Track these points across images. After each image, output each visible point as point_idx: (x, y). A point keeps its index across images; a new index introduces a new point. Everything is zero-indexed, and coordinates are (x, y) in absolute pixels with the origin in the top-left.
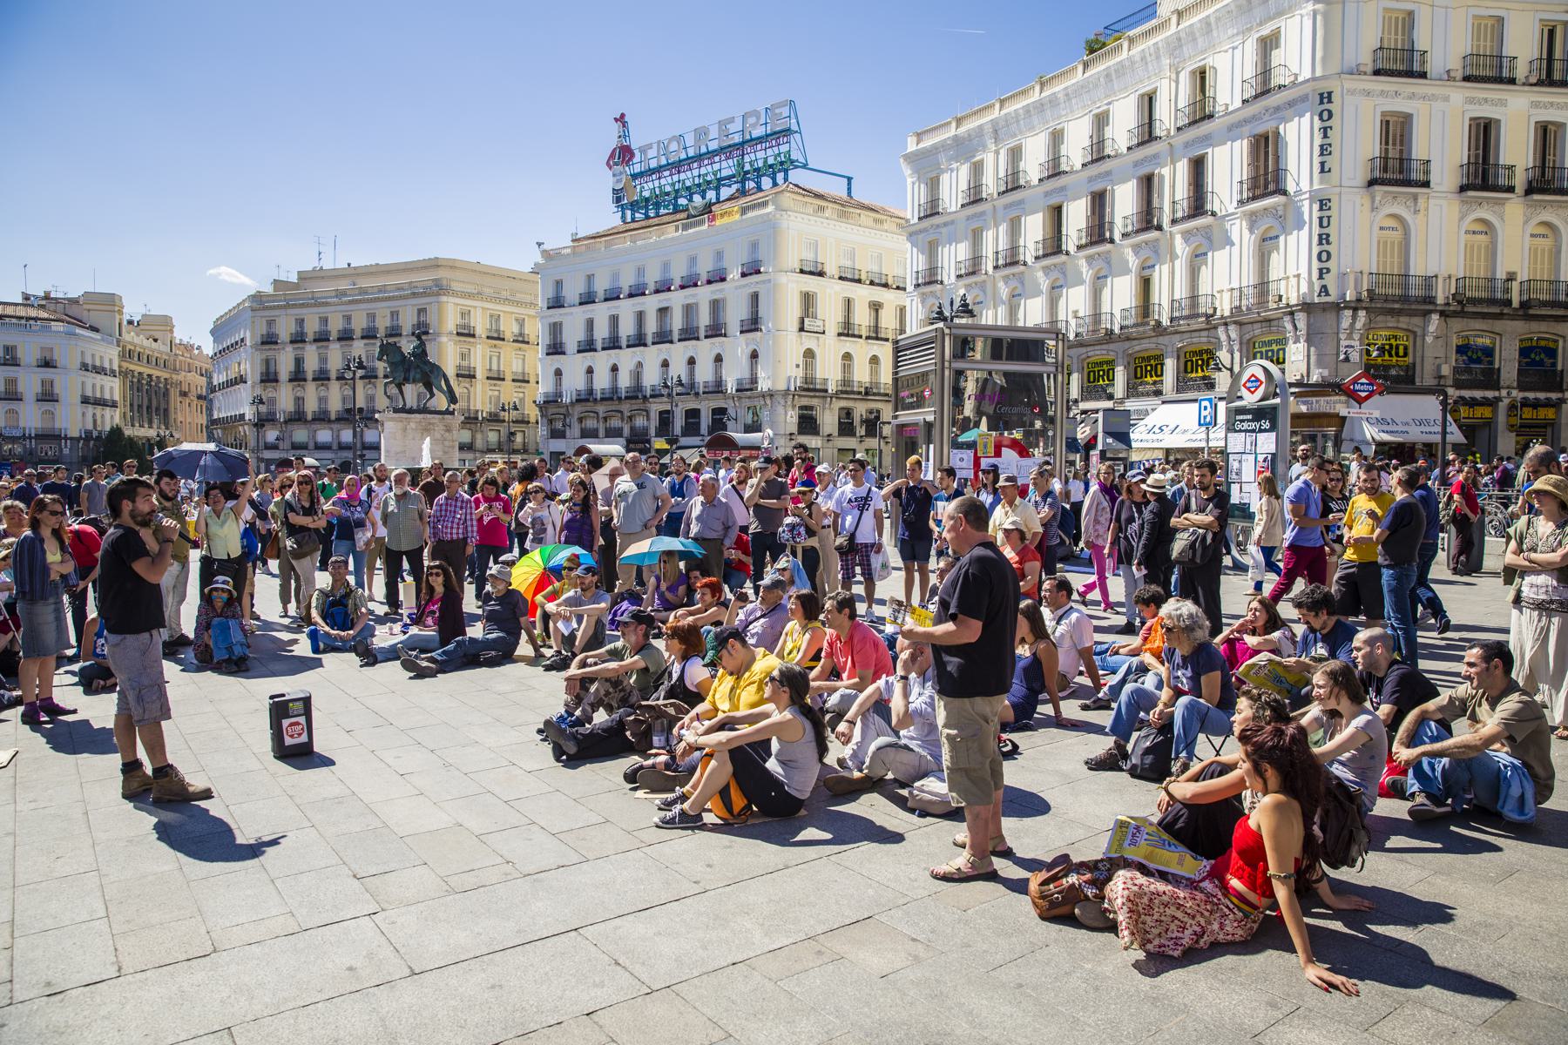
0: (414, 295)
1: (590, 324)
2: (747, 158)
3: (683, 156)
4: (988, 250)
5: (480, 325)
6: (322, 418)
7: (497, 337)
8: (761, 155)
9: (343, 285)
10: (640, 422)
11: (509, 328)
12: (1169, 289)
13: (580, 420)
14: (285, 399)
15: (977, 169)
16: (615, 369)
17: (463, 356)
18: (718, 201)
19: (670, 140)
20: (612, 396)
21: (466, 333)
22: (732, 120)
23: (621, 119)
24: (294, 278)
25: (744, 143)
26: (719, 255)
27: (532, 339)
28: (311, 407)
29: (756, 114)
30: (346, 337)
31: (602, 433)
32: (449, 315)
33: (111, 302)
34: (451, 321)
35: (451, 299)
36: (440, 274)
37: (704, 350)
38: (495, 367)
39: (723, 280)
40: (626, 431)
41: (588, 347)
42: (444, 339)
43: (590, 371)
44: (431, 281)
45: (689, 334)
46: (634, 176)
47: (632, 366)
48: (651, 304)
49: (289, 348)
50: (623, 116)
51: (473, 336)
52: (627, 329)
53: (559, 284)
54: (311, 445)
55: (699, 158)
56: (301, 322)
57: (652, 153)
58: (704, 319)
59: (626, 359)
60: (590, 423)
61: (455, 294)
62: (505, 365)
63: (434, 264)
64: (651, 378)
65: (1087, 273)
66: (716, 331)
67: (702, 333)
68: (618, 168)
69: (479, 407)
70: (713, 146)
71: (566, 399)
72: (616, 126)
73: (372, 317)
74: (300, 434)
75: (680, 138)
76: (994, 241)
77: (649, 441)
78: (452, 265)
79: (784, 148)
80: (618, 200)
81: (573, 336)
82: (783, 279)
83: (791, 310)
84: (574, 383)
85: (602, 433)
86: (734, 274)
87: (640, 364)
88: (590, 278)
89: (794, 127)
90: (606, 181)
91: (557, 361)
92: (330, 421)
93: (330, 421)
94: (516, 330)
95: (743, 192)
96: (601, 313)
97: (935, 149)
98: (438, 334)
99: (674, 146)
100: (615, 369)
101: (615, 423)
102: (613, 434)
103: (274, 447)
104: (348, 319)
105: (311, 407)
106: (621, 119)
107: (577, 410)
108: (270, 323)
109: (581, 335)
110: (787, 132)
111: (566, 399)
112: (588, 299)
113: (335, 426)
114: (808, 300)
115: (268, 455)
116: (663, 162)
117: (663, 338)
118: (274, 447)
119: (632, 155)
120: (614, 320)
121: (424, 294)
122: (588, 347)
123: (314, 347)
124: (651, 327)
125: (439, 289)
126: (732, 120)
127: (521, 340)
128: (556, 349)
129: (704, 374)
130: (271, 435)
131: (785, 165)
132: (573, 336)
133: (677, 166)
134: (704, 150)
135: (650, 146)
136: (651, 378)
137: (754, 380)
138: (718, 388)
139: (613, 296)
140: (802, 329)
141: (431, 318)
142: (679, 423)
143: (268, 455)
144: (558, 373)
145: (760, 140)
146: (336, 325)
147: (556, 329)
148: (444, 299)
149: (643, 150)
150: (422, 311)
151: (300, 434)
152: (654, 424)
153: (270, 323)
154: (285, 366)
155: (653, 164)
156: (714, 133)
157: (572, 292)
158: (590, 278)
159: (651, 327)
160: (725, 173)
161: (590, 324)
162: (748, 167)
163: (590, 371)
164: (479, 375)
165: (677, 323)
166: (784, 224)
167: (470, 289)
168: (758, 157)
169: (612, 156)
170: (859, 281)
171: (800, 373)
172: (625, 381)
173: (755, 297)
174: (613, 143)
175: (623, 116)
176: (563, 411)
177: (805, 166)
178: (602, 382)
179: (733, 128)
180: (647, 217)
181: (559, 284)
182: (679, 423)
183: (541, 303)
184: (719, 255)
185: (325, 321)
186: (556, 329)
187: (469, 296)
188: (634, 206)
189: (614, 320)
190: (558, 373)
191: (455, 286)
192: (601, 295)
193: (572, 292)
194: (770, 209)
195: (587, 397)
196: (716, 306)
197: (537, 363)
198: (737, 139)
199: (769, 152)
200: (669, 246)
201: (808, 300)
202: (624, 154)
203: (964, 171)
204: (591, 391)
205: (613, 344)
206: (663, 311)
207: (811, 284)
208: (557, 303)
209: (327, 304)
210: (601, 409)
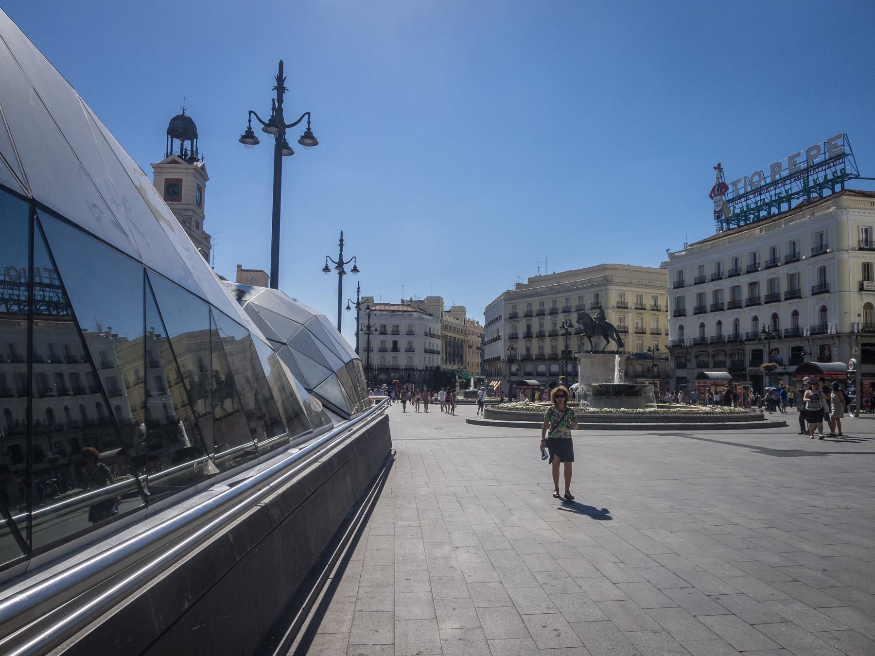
0: (592, 286)
2: (811, 178)
3: (763, 183)
5: (631, 301)
6: (541, 358)
7: (641, 308)
8: (823, 173)
9: (553, 284)
11: (648, 302)
13: (697, 357)
14: (521, 348)
19: (753, 175)
20: (718, 341)
23: (719, 168)
24: (526, 282)
25: (807, 168)
27: (663, 308)
28: (535, 352)
29: (817, 148)
30: (554, 312)
31: (711, 365)
35: (613, 287)
36: (607, 273)
37: (785, 310)
38: (640, 326)
40: (728, 363)
41: (700, 310)
42: (610, 311)
43: (702, 325)
44: (601, 277)
45: (773, 298)
46: (729, 201)
47: (732, 320)
49: (524, 320)
50: (719, 165)
51: (627, 308)
53: (681, 273)
54: (535, 373)
55: (775, 183)
58: (784, 288)
59: (728, 318)
61: (616, 284)
63: (603, 268)
64: (746, 328)
66: (794, 294)
67: (783, 297)
68: (718, 198)
70: (785, 173)
74: (529, 367)
75: (759, 173)
77: (745, 370)
78: (613, 267)
81: (690, 305)
84: (692, 333)
85: (711, 365)
88: (701, 267)
89: (848, 151)
90: (710, 206)
91: (681, 321)
92: (545, 360)
93: (545, 360)
94: (652, 303)
96: (709, 288)
101: (721, 358)
102: (718, 366)
103: (515, 374)
104: (555, 302)
105: (535, 352)
108: (514, 307)
110: (842, 156)
111: (687, 343)
112: (700, 281)
113: (548, 363)
116: (749, 189)
118: (515, 374)
119: (727, 188)
121: (598, 286)
122: (700, 310)
123: (537, 319)
125: (607, 282)
127: (656, 308)
128: (679, 313)
129: (785, 324)
131: (843, 177)
132: (690, 305)
133: (759, 191)
134: (777, 177)
135: (739, 181)
137: (824, 327)
138: (796, 333)
140: (861, 289)
144: (681, 328)
145: (820, 164)
146: (548, 306)
148: (610, 287)
149: (734, 184)
150: (597, 296)
151: (529, 367)
152: (748, 358)
153: (514, 307)
154: (521, 330)
155: (742, 192)
156: (785, 165)
158: (701, 267)
160: (794, 190)
162: (811, 184)
163: (702, 325)
164: (631, 330)
166: (845, 218)
167: (625, 280)
171: (862, 320)
173: (823, 271)
174: (714, 183)
175: (719, 165)
176: (684, 351)
177: (857, 177)
178: (711, 332)
179: (798, 160)
180: (739, 226)
181: (681, 273)
183: (669, 285)
185: (542, 304)
186: (679, 301)
190: (681, 328)
191: (615, 279)
195: (701, 342)
197: (665, 321)
199: (828, 171)
202: (721, 188)
204: (703, 338)
206: (753, 285)
209: (544, 295)
210: (711, 350)
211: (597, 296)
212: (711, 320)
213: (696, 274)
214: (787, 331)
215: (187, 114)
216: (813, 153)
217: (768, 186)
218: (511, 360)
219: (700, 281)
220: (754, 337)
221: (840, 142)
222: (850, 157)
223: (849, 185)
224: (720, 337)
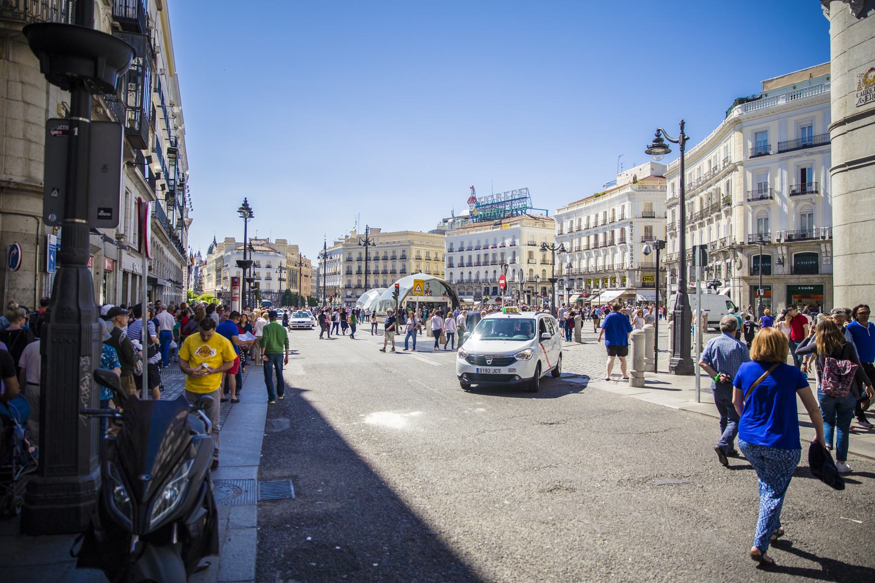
1: (462, 258)
4: (574, 246)
5: (423, 255)
7: (428, 259)
10: (478, 290)
12: (609, 262)
14: (354, 280)
15: (572, 222)
16: (470, 273)
18: (504, 218)
21: (418, 258)
23: (472, 188)
27: (441, 259)
33: (283, 242)
34: (414, 255)
36: (410, 238)
41: (462, 265)
43: (462, 273)
48: (482, 252)
52: (474, 260)
53: (452, 244)
61: (416, 245)
63: (406, 233)
64: (482, 276)
65: (586, 257)
71: (454, 283)
72: (471, 191)
73: (386, 252)
76: (576, 243)
78: (412, 234)
81: (456, 261)
82: (522, 247)
83: (526, 257)
84: (456, 277)
95: (512, 216)
97: (561, 215)
99: (490, 199)
100: (470, 273)
101: (470, 291)
102: (469, 294)
103: (350, 297)
104: (377, 253)
106: (472, 188)
108: (350, 254)
109: (459, 262)
111: (454, 283)
114: (531, 254)
115: (348, 300)
117: (486, 264)
118: (350, 297)
120: (470, 257)
122: (462, 265)
124: (482, 260)
125: (411, 243)
127: (436, 259)
128: (451, 266)
130: (349, 293)
132: (456, 261)
136: (482, 276)
139: (470, 249)
141: (407, 254)
142: (491, 291)
143: (348, 300)
144: (451, 274)
147: (450, 259)
150: (404, 251)
152: (483, 291)
153: (350, 254)
154: (355, 269)
156: (503, 196)
157: (456, 247)
158: (462, 243)
159: (482, 260)
161: (462, 258)
163: (462, 273)
168: (516, 205)
172: (473, 277)
174: (470, 196)
178: (466, 277)
181: (452, 244)
182: (491, 291)
186: (450, 259)
187: (420, 245)
189: (470, 257)
190: (451, 274)
193: (456, 247)
194: (518, 226)
197: (443, 267)
201: (531, 254)
202: (473, 199)
204: (462, 280)
205: (470, 265)
206: (486, 255)
207: (532, 248)
208: (451, 250)
211: (404, 251)
212: (466, 270)
213: (459, 246)
218: (348, 287)
219: (461, 250)
220: (486, 281)
223: (528, 211)
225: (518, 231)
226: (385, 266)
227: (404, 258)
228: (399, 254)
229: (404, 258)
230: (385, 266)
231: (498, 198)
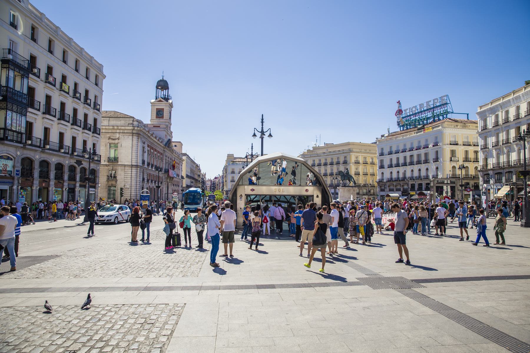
0: (343, 153)
1: (391, 160)
2: (435, 112)
3: (417, 112)
4: (501, 139)
5: (361, 160)
7: (365, 163)
8: (439, 110)
9: (325, 151)
10: (406, 187)
11: (369, 160)
13: (389, 186)
15: (497, 116)
16: (398, 172)
17: (356, 169)
18: (427, 124)
19: (413, 107)
20: (398, 179)
21: (357, 163)
22: (430, 101)
23: (399, 102)
24: (312, 149)
25: (434, 108)
26: (427, 140)
29: (437, 99)
31: (395, 190)
32: (353, 158)
34: (353, 159)
36: (350, 147)
37: (423, 167)
39: (428, 147)
40: (402, 189)
41: (391, 166)
43: (391, 173)
44: (347, 149)
45: (419, 162)
46: (403, 118)
47: (403, 171)
48: (408, 154)
52: (401, 161)
53: (382, 149)
55: (421, 112)
56: (314, 161)
57: (408, 111)
58: (423, 158)
59: (401, 169)
60: (392, 187)
61: (354, 152)
62: (368, 171)
63: (348, 144)
65: (516, 148)
66: (426, 161)
67: (422, 162)
69: (361, 182)
70: (425, 109)
71: (385, 181)
72: (397, 104)
73: (332, 159)
75: (415, 107)
76: (502, 136)
78: (353, 144)
79: (446, 108)
80: (399, 125)
81: (386, 163)
82: (445, 147)
83: (448, 155)
84: (387, 176)
85: (395, 190)
86: (430, 146)
87: (405, 171)
88: (391, 147)
89: (448, 102)
90: (395, 119)
91: (382, 170)
94: (371, 161)
95: (434, 121)
96: (394, 157)
97: (484, 111)
98: (350, 163)
99: (414, 109)
100: (398, 172)
101: (398, 187)
102: (398, 190)
104: (326, 160)
106: (399, 102)
107: (388, 184)
109: (389, 163)
110: (446, 104)
111: (385, 181)
112: (390, 153)
114: (453, 153)
116: (411, 113)
117: (412, 163)
120: (398, 159)
121: (346, 153)
122: (391, 166)
124: (408, 160)
125: (350, 151)
126: (430, 101)
127: (373, 163)
128: (382, 167)
129: (423, 173)
131: (447, 113)
132: (386, 163)
133: (415, 114)
134: (422, 110)
135: (407, 109)
136: (408, 175)
137: (437, 175)
138: (427, 177)
139: (397, 152)
140: (451, 160)
141: (348, 159)
144: (383, 173)
145: (438, 106)
146: (323, 162)
149: (405, 110)
150: (345, 157)
152: (410, 186)
155: (408, 114)
156: (425, 105)
157: (386, 151)
158: (391, 147)
159: (408, 160)
160: (429, 116)
161: (391, 160)
162: (435, 114)
163: (391, 173)
164: (361, 174)
165: (415, 159)
166: (445, 131)
167: (358, 150)
168: (437, 111)
169: (397, 112)
170: (470, 145)
171: (451, 173)
172: (401, 176)
173: (437, 152)
174: (397, 109)
177: (452, 113)
178: (395, 176)
179: (430, 103)
180: (407, 129)
181: (382, 149)
182: (416, 187)
183: (377, 155)
184: (427, 140)
185: (320, 160)
186: (382, 161)
187: (358, 152)
188: (403, 126)
189: (398, 159)
190: (383, 173)
191: (354, 150)
192: (394, 152)
193: (386, 151)
194: (440, 128)
195: (390, 180)
196: (426, 155)
197: (376, 169)
198: (432, 106)
199: (442, 110)
200: (413, 137)
201: (453, 153)
202: (400, 112)
203: (493, 117)
204: (391, 178)
205: (398, 165)
206: (411, 156)
207: (454, 147)
208: (382, 154)
210: (395, 183)
211: (345, 157)
212: (395, 170)
213: (388, 150)
214: (424, 176)
215: (164, 79)
216: (436, 101)
217: (418, 113)
219: (390, 153)
220: (412, 178)
221: (445, 98)
222: (449, 105)
223: (449, 116)
224: (398, 178)
225: (441, 133)
226: (332, 170)
227: (345, 162)
228: (342, 160)
229: (345, 162)
230: (332, 170)
231: (420, 107)
